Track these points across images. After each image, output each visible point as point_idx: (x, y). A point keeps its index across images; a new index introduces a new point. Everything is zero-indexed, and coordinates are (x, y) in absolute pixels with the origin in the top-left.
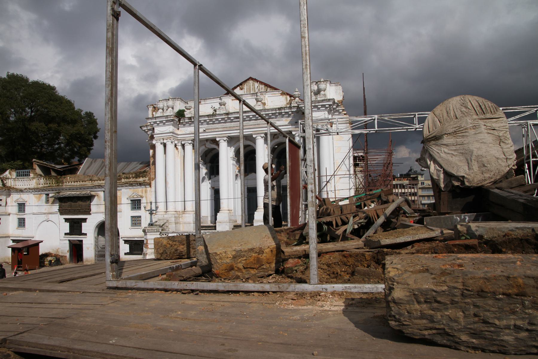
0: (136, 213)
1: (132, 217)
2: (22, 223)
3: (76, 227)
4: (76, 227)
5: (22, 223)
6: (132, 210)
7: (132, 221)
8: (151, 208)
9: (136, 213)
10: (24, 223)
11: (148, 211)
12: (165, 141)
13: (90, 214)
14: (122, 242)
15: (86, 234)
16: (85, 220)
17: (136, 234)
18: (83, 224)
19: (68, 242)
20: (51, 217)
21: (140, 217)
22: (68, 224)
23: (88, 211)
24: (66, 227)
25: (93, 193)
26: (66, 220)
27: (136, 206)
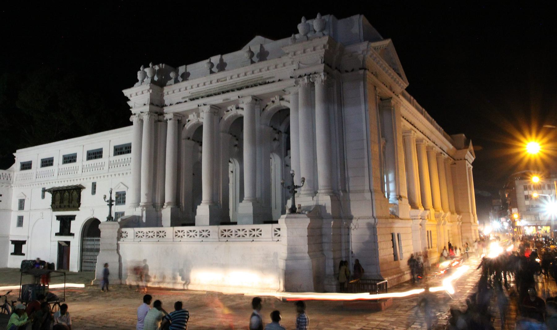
8: (111, 198)
11: (107, 201)
15: (73, 235)
16: (73, 218)
22: (59, 222)
24: (57, 225)
25: (83, 185)
26: (58, 218)
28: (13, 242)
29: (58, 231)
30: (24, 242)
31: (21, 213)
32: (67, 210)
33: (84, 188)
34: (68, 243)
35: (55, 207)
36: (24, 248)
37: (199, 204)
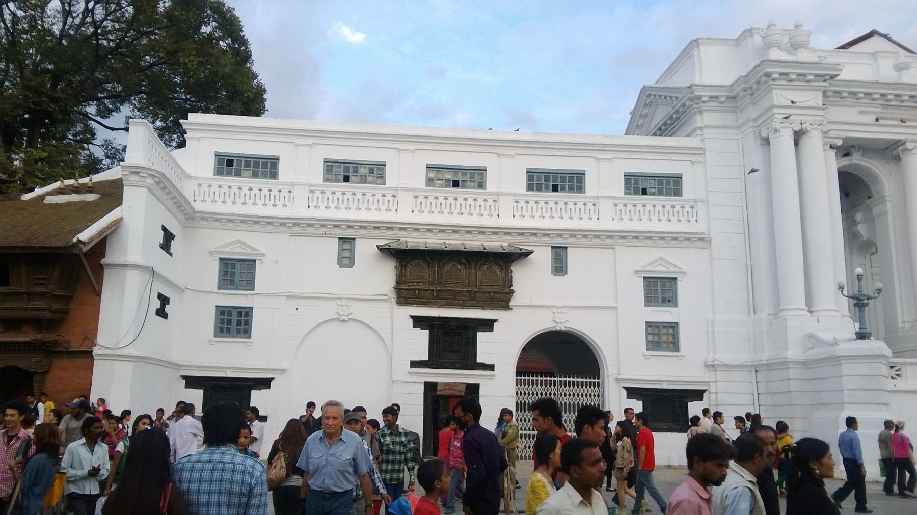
0: (662, 314)
1: (649, 324)
2: (234, 323)
3: (453, 343)
4: (453, 343)
6: (646, 305)
7: (647, 334)
9: (662, 314)
10: (248, 323)
15: (491, 367)
16: (488, 325)
17: (664, 372)
18: (481, 337)
21: (674, 326)
22: (424, 335)
23: (502, 298)
24: (419, 343)
26: (419, 322)
27: (660, 296)
28: (191, 382)
29: (425, 357)
32: (462, 306)
34: (473, 389)
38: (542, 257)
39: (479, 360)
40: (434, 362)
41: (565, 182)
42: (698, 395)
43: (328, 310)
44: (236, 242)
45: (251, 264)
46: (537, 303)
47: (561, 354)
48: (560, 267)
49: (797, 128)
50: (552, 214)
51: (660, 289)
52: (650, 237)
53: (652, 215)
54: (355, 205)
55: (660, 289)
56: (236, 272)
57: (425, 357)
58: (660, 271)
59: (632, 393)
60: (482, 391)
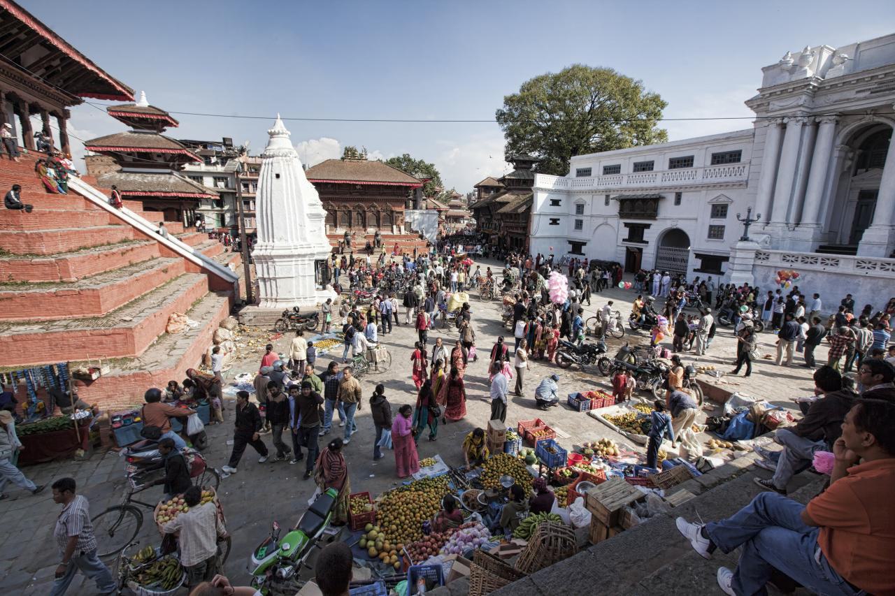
0: (718, 222)
1: (711, 227)
2: (579, 224)
3: (636, 233)
4: (636, 233)
5: (579, 224)
8: (748, 217)
9: (718, 222)
10: (581, 225)
12: (785, 121)
13: (655, 219)
14: (692, 257)
15: (647, 242)
16: (648, 226)
17: (714, 247)
18: (646, 231)
19: (625, 249)
20: (610, 221)
22: (627, 229)
23: (653, 215)
24: (625, 233)
25: (663, 195)
26: (626, 225)
28: (570, 242)
29: (627, 237)
30: (585, 244)
31: (580, 217)
33: (664, 198)
34: (640, 250)
35: (622, 214)
36: (584, 249)
37: (867, 228)
38: (671, 198)
39: (645, 239)
40: (630, 239)
41: (687, 162)
42: (726, 259)
43: (601, 221)
44: (576, 198)
45: (583, 206)
46: (669, 217)
47: (676, 238)
48: (678, 202)
49: (779, 121)
50: (681, 177)
51: (719, 210)
52: (715, 186)
53: (726, 172)
54: (612, 182)
55: (719, 210)
56: (580, 208)
57: (627, 237)
58: (722, 201)
59: (698, 256)
60: (644, 251)
